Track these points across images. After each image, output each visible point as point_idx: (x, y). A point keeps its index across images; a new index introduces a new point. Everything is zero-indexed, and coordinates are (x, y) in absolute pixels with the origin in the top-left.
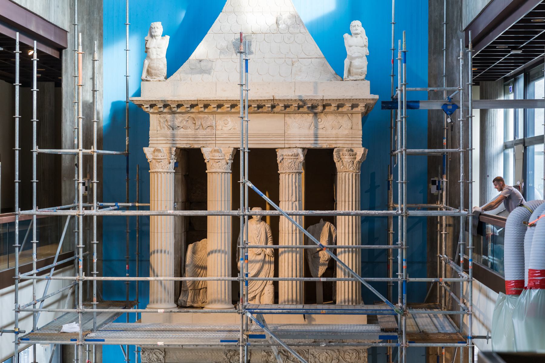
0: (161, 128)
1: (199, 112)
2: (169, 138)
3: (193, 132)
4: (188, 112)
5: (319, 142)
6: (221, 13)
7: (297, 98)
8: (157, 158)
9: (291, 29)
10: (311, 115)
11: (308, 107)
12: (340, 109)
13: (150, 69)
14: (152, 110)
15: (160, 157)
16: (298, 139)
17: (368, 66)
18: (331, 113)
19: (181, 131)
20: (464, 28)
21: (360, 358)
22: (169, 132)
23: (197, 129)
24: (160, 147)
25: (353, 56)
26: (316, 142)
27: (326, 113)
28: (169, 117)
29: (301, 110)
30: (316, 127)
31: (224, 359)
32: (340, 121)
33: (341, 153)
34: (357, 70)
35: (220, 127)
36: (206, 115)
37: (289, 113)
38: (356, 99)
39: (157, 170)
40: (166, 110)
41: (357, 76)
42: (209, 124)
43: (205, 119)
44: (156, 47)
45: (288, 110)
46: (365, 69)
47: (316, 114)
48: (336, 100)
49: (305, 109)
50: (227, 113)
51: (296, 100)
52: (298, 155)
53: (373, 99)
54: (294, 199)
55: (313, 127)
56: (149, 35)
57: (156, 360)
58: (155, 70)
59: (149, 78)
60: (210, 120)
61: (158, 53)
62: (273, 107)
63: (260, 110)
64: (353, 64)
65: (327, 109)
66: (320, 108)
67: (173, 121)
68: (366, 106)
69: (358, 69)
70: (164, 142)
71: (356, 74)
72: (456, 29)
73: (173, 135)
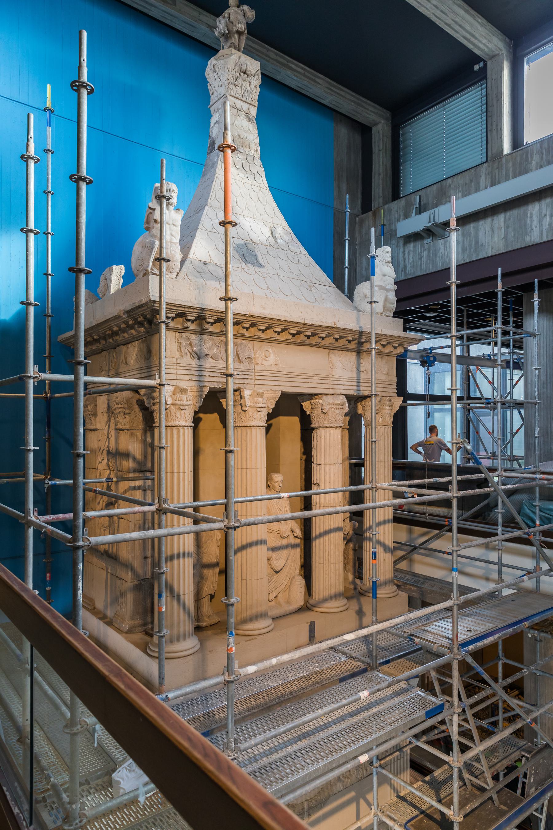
2: (194, 373)
5: (361, 388)
6: (207, 207)
8: (181, 403)
15: (185, 402)
16: (342, 383)
19: (209, 363)
22: (194, 362)
24: (183, 384)
26: (358, 388)
28: (193, 337)
35: (260, 361)
36: (244, 341)
39: (177, 423)
40: (192, 326)
42: (247, 354)
43: (242, 346)
50: (272, 341)
67: (200, 345)
70: (187, 377)
73: (200, 367)
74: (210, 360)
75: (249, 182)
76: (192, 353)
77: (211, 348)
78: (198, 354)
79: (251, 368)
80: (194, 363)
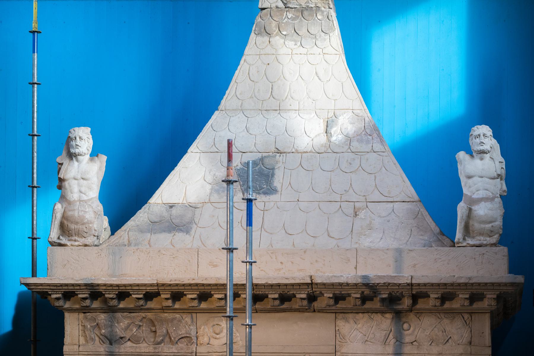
0: (87, 341)
1: (164, 309)
3: (151, 349)
4: (139, 309)
6: (216, 113)
7: (359, 281)
9: (355, 144)
10: (389, 316)
11: (383, 300)
12: (447, 305)
13: (65, 222)
14: (67, 305)
17: (506, 217)
19: (128, 347)
23: (159, 343)
25: (475, 196)
27: (420, 313)
28: (102, 317)
29: (368, 305)
30: (399, 341)
32: (447, 329)
34: (483, 226)
36: (178, 316)
37: (344, 312)
38: (479, 284)
40: (96, 304)
41: (482, 238)
42: (182, 332)
43: (175, 322)
44: (79, 177)
45: (341, 305)
46: (499, 223)
47: (398, 315)
48: (438, 285)
49: (376, 304)
51: (356, 285)
53: (512, 284)
55: (392, 340)
56: (64, 153)
58: (77, 223)
59: (64, 241)
60: (185, 325)
61: (83, 189)
62: (312, 298)
63: (286, 305)
64: (475, 213)
65: (421, 304)
66: (407, 302)
67: (111, 326)
68: (498, 298)
71: (481, 234)
74: (129, 344)
75: (303, 51)
76: (101, 337)
77: (127, 328)
78: (109, 337)
79: (190, 351)
80: (102, 349)
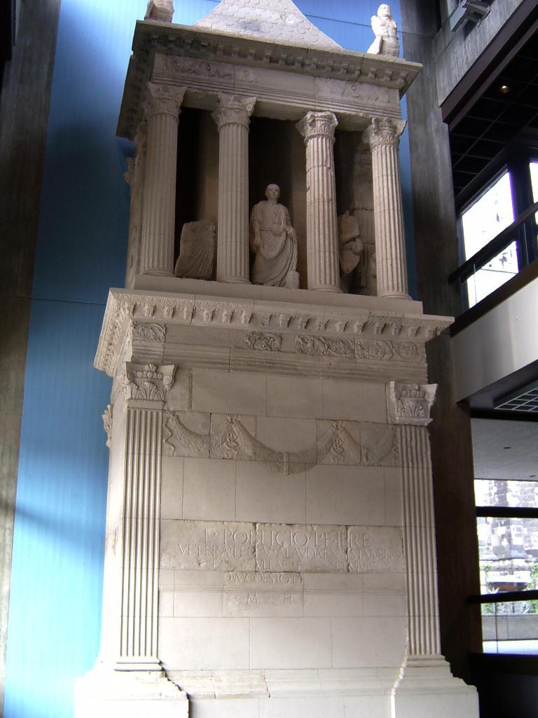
9: (300, 25)
13: (155, 11)
15: (167, 97)
18: (368, 83)
20: (441, 101)
21: (417, 354)
27: (361, 83)
31: (246, 343)
33: (381, 124)
52: (330, 118)
54: (329, 166)
57: (152, 337)
60: (228, 69)
69: (389, 47)
72: (433, 105)
